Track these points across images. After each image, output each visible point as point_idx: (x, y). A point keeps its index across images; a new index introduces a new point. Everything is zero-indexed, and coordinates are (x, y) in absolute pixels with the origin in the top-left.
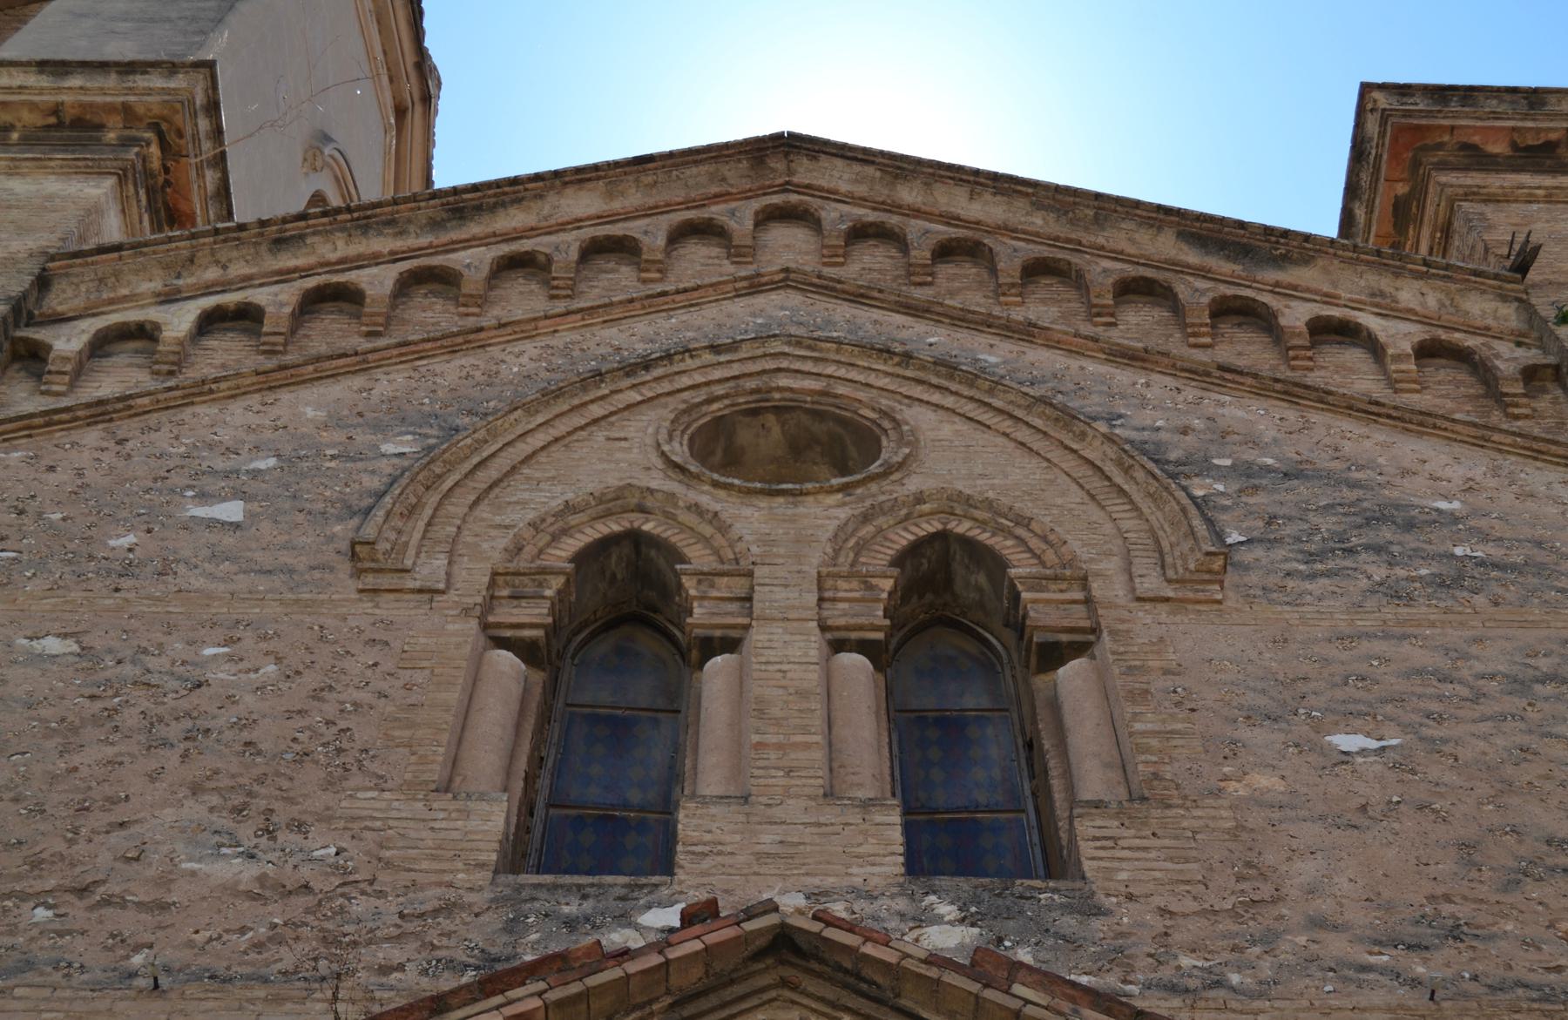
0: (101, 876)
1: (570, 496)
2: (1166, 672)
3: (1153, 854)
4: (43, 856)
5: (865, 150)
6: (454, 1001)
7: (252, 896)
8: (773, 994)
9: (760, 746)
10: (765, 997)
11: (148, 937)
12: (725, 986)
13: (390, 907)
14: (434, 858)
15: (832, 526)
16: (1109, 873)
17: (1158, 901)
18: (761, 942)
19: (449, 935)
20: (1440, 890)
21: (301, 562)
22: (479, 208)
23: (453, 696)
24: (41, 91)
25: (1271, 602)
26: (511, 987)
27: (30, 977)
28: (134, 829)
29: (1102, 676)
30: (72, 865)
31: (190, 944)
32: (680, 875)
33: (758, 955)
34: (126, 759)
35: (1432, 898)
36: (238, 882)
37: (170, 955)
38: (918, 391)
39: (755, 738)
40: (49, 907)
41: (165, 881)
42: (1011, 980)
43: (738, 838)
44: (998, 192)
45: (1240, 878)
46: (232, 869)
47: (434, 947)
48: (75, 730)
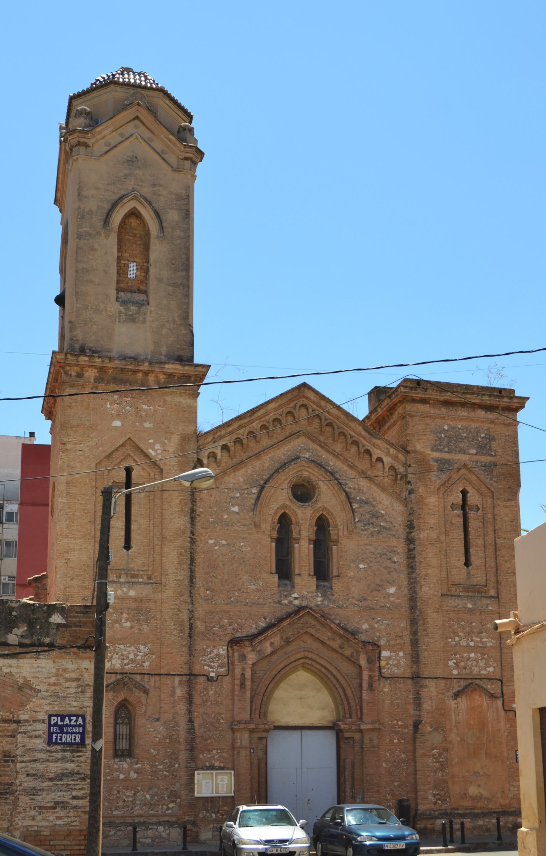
1: (278, 506)
2: (345, 552)
5: (318, 392)
15: (310, 515)
21: (248, 523)
22: (257, 411)
23: (269, 555)
24: (181, 370)
29: (338, 550)
38: (321, 477)
44: (337, 409)
46: (253, 587)
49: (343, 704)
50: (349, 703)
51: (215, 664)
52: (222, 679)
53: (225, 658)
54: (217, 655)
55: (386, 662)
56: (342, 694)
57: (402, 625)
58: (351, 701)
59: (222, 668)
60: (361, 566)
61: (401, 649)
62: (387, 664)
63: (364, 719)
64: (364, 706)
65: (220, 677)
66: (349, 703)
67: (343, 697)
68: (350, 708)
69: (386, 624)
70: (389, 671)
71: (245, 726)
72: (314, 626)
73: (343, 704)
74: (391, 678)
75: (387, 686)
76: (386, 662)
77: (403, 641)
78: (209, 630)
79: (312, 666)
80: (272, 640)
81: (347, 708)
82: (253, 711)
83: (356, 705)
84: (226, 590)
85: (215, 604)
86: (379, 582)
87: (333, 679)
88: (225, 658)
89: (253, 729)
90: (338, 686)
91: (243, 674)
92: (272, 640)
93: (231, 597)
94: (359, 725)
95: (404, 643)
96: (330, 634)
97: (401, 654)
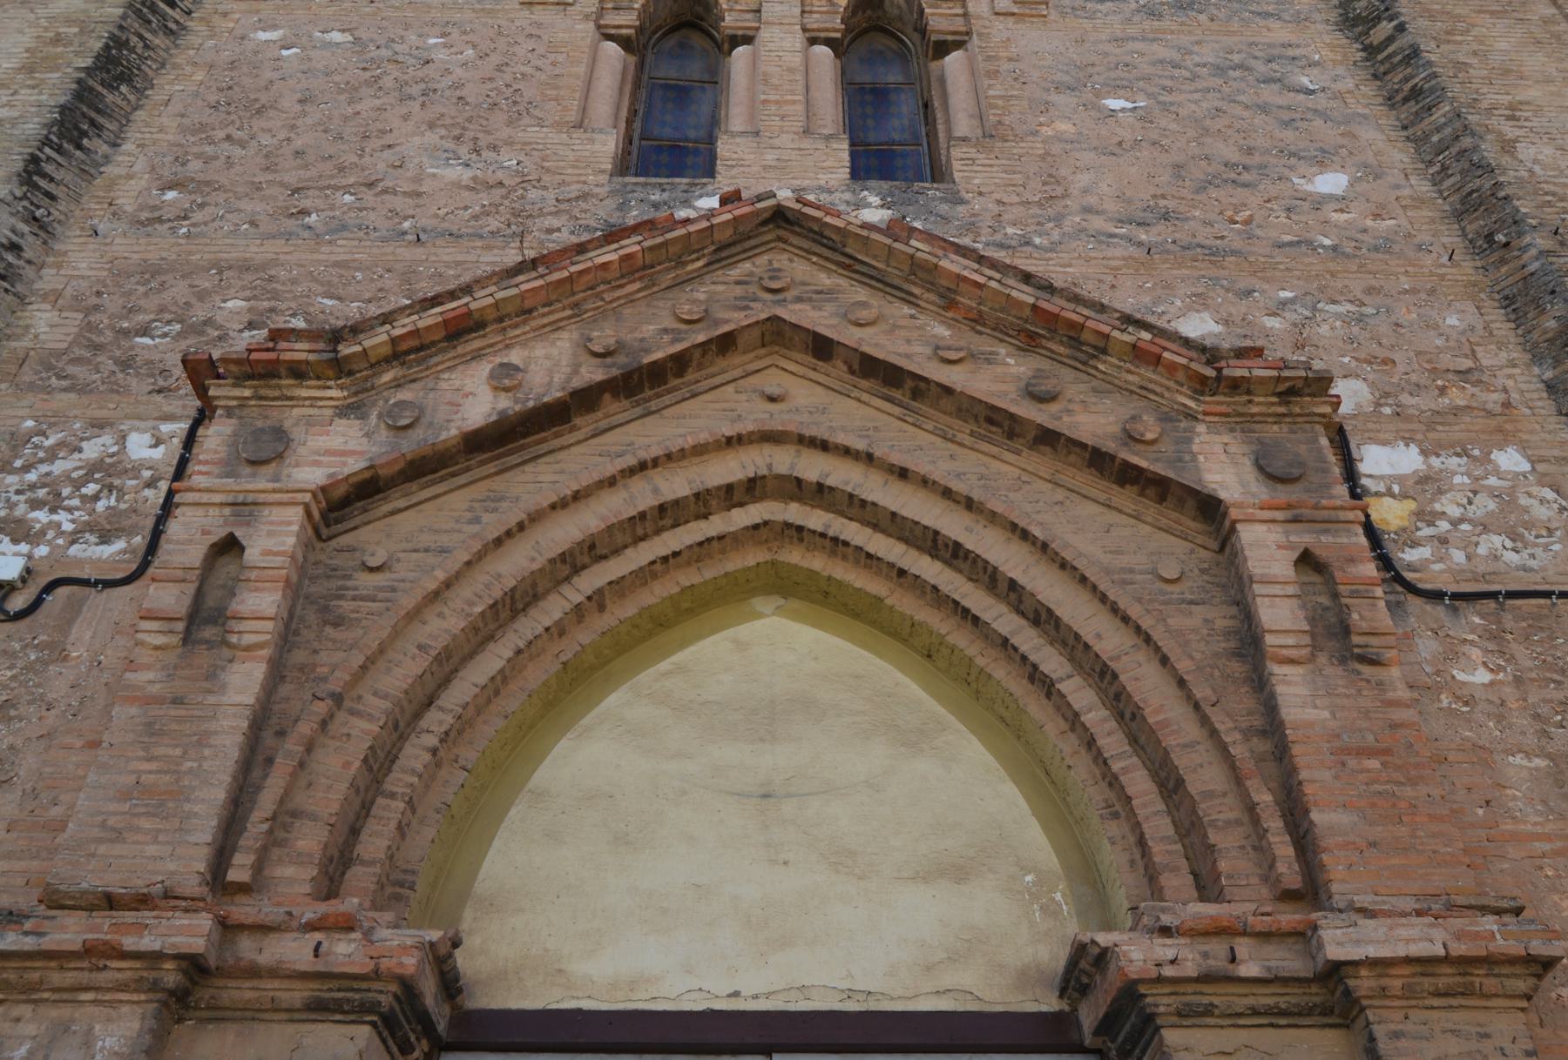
0: (380, 177)
2: (1010, 59)
3: (995, 169)
4: (346, 164)
6: (590, 247)
7: (472, 189)
8: (773, 245)
9: (765, 102)
10: (769, 246)
11: (411, 212)
12: (745, 240)
13: (551, 195)
14: (574, 167)
16: (968, 180)
17: (997, 196)
18: (766, 215)
19: (585, 211)
20: (1159, 192)
23: (581, 70)
25: (1076, 16)
26: (623, 239)
27: (345, 234)
28: (397, 149)
29: (971, 62)
30: (363, 170)
31: (436, 216)
32: (719, 178)
33: (765, 223)
34: (388, 107)
35: (1154, 196)
36: (460, 181)
37: (424, 222)
39: (763, 97)
40: (352, 194)
41: (418, 179)
42: (909, 238)
43: (752, 156)
45: (1044, 184)
46: (455, 173)
47: (577, 219)
48: (356, 89)
49: (1121, 803)
50: (1171, 785)
51: (62, 517)
52: (74, 609)
53: (151, 484)
54: (93, 468)
55: (1411, 505)
56: (1096, 716)
57: (1452, 320)
58: (1181, 760)
59: (105, 539)
60: (1114, 104)
61: (1504, 438)
62: (1426, 516)
63: (1342, 881)
64: (1315, 775)
65: (63, 591)
66: (1171, 785)
67: (1112, 741)
68: (1190, 828)
69: (1338, 316)
70: (1458, 556)
71: (101, 927)
72: (827, 294)
73: (1121, 803)
74: (1493, 595)
75: (1476, 654)
76: (1411, 505)
77: (1497, 396)
78: (98, 347)
79: (837, 545)
80: (515, 357)
81: (1159, 826)
82: (256, 827)
83: (1237, 778)
84: (282, 184)
85: (188, 236)
86: (1235, 157)
87: (1003, 619)
88: (151, 484)
89: (195, 967)
90: (1052, 662)
91: (229, 546)
92: (515, 357)
93: (304, 212)
94: (1304, 936)
95: (1507, 405)
96: (943, 331)
97: (1510, 460)
